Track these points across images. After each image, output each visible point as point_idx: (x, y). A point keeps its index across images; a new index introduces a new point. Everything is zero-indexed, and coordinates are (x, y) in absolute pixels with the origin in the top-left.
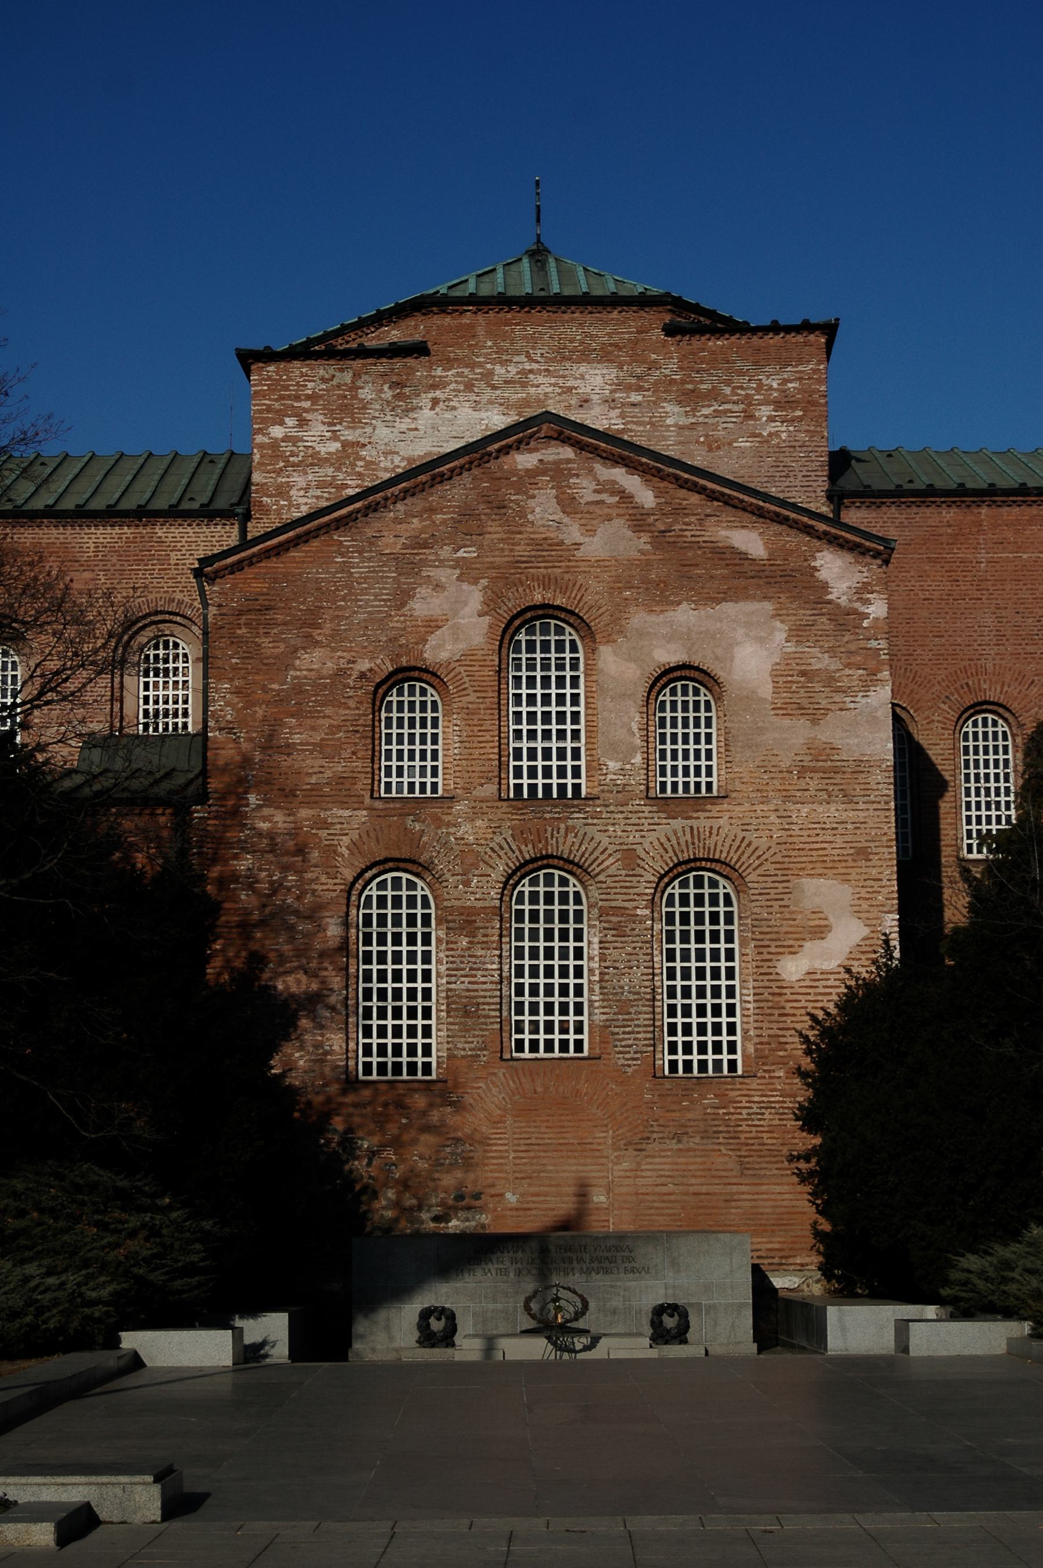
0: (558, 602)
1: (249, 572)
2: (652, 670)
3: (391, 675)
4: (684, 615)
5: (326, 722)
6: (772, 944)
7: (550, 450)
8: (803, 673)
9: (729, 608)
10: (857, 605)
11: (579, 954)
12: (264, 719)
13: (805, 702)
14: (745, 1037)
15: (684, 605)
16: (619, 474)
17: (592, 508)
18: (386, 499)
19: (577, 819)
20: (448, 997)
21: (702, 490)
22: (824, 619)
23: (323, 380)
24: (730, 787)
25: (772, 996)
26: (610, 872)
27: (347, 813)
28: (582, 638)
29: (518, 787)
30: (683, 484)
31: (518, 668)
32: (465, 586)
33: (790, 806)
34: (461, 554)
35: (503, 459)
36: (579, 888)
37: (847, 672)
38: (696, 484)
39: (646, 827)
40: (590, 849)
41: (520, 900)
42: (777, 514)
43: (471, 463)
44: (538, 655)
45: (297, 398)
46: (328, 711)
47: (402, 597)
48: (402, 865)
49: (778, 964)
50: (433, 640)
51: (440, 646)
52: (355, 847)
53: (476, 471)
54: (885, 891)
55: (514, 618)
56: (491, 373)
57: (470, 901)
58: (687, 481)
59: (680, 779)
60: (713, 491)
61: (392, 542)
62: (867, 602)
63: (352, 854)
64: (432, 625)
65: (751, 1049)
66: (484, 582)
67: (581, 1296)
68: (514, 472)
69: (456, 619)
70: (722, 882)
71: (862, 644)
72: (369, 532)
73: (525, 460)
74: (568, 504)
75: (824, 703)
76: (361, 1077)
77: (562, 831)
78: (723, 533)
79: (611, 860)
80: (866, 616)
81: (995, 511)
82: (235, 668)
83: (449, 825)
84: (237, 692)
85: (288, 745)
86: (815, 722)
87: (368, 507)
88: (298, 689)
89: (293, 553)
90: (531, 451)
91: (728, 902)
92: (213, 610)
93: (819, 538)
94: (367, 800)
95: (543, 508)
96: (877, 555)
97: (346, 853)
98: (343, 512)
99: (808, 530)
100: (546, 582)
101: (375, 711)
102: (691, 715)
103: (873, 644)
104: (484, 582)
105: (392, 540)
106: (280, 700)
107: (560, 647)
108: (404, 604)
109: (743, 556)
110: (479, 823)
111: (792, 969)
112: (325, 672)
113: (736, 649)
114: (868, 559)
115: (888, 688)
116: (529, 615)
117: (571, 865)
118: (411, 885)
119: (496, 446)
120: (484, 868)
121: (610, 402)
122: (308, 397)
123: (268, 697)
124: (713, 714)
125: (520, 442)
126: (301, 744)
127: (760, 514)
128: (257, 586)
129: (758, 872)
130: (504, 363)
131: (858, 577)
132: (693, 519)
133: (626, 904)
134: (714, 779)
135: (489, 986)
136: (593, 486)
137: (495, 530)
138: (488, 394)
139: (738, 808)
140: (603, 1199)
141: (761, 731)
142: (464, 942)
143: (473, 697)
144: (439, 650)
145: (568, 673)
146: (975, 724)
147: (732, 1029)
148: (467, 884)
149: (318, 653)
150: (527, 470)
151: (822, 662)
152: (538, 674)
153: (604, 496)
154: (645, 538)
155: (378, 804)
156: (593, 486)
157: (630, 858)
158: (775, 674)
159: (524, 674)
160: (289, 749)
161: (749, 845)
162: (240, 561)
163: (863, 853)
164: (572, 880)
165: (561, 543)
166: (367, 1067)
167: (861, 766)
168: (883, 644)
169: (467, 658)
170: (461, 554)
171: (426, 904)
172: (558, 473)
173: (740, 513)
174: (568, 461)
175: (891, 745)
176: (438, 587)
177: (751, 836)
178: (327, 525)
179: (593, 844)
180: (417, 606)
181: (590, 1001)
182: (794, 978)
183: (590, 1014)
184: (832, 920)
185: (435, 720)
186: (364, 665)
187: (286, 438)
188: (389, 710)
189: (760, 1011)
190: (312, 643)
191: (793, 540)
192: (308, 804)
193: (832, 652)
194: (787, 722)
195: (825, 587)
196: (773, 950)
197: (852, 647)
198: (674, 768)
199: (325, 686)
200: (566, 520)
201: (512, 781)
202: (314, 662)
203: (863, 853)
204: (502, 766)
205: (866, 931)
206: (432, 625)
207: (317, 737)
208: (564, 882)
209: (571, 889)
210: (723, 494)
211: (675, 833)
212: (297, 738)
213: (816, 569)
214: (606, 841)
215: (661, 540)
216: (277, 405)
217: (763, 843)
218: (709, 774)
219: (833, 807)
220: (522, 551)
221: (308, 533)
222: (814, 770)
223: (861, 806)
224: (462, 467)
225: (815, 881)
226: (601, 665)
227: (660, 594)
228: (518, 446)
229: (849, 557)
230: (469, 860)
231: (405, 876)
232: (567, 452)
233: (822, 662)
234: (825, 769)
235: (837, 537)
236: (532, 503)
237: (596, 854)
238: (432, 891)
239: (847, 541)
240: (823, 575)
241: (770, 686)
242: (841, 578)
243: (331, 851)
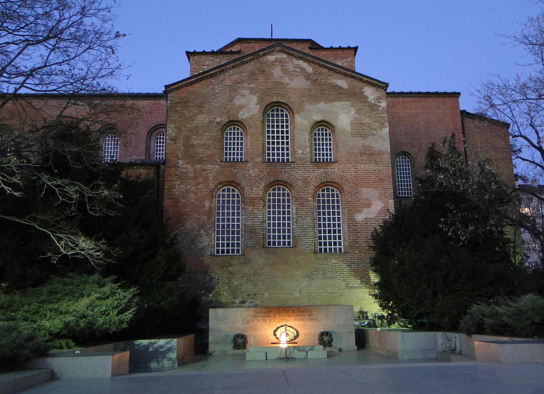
0: (282, 101)
1: (182, 90)
2: (312, 122)
3: (227, 123)
4: (322, 105)
5: (206, 138)
6: (353, 209)
7: (280, 55)
8: (361, 124)
9: (337, 104)
10: (377, 103)
11: (289, 213)
12: (185, 136)
13: (361, 133)
14: (345, 240)
15: (322, 103)
16: (301, 63)
17: (294, 73)
18: (226, 68)
19: (288, 169)
20: (245, 227)
21: (327, 68)
22: (367, 107)
23: (211, 61)
24: (338, 159)
25: (354, 227)
26: (299, 186)
27: (212, 166)
28: (289, 113)
29: (269, 159)
30: (321, 66)
31: (269, 122)
32: (252, 96)
33: (357, 165)
34: (250, 86)
35: (264, 57)
36: (289, 192)
37: (375, 123)
38: (325, 66)
39: (311, 171)
40: (293, 178)
41: (269, 195)
42: (351, 75)
43: (254, 58)
44: (275, 118)
45: (203, 65)
46: (207, 134)
47: (231, 99)
48: (230, 184)
49: (355, 216)
50: (241, 112)
51: (244, 114)
52: (215, 178)
53: (256, 61)
54: (389, 192)
55: (267, 106)
57: (253, 195)
58: (322, 65)
60: (331, 68)
61: (228, 82)
62: (380, 102)
63: (213, 179)
64: (241, 107)
65: (347, 244)
66: (258, 94)
67: (296, 330)
68: (267, 61)
69: (249, 106)
70: (335, 190)
71: (379, 115)
72: (221, 78)
73: (271, 58)
74: (285, 71)
75: (367, 133)
76: (216, 254)
77: (283, 172)
78: (334, 81)
79: (300, 182)
80: (380, 106)
81: (404, 99)
82: (176, 120)
83: (246, 170)
84: (176, 128)
85: (193, 145)
86: (365, 139)
87: (221, 71)
88: (197, 127)
90: (273, 55)
91: (338, 196)
92: (169, 102)
93: (364, 83)
94: (219, 162)
95: (277, 72)
96: (383, 88)
97: (211, 179)
98: (213, 72)
99: (361, 80)
100: (278, 95)
101: (222, 134)
102: (325, 137)
103: (382, 115)
104: (258, 94)
105: (228, 81)
106: (191, 130)
107: (282, 116)
108: (232, 101)
109: (341, 88)
111: (360, 217)
112: (205, 122)
113: (339, 116)
114: (380, 89)
115: (388, 129)
116: (272, 105)
117: (286, 184)
118: (233, 191)
119: (262, 53)
120: (257, 184)
122: (207, 65)
123: (187, 129)
124: (331, 137)
125: (269, 52)
126: (197, 144)
127: (346, 75)
128: (184, 95)
129: (348, 185)
131: (377, 95)
132: (324, 76)
133: (305, 196)
134: (332, 157)
135: (259, 223)
136: (293, 66)
137: (261, 79)
139: (341, 166)
140: (298, 295)
142: (251, 208)
143: (254, 130)
144: (243, 115)
145: (285, 124)
146: (400, 158)
147: (340, 238)
148: (252, 189)
149: (204, 116)
150: (272, 61)
151: (367, 120)
153: (296, 69)
154: (309, 82)
155: (223, 164)
156: (293, 66)
157: (306, 181)
158: (351, 124)
159: (271, 124)
160: (193, 146)
161: (345, 177)
162: (178, 87)
163: (381, 180)
164: (287, 189)
165: (283, 83)
166: (218, 251)
167: (380, 153)
168: (386, 115)
169: (251, 118)
170: (250, 86)
171: (238, 197)
172: (281, 62)
173: (340, 75)
174: (285, 58)
175: (389, 146)
176: (243, 96)
177: (345, 174)
178: (207, 76)
179: (294, 177)
180: (236, 101)
181: (293, 228)
182: (360, 220)
183: (293, 233)
184: (372, 202)
185: (242, 138)
186: (218, 120)
188: (227, 135)
189: (349, 232)
190: (201, 112)
192: (200, 163)
193: (369, 117)
194: (356, 139)
195: (367, 97)
196: (353, 211)
197: (376, 116)
198: (319, 154)
199: (205, 126)
200: (284, 76)
201: (267, 158)
202: (202, 119)
203: (381, 180)
204: (264, 152)
205: (383, 205)
206: (241, 107)
207: (203, 142)
208: (284, 190)
209: (286, 192)
210: (334, 69)
211: (320, 173)
212: (196, 142)
213: (363, 92)
214: (298, 176)
215: (315, 82)
216: (197, 67)
217: (349, 177)
218: (331, 156)
219: (371, 165)
220: (270, 85)
221: (201, 78)
223: (380, 165)
224: (251, 59)
226: (295, 120)
227: (315, 99)
228: (269, 53)
229: (374, 89)
230: (253, 182)
231: (231, 188)
232: (285, 56)
233: (367, 120)
234: (369, 154)
235: (370, 82)
236: (273, 71)
237: (295, 180)
238: (240, 192)
239: (374, 84)
240: (366, 94)
241: (350, 128)
242: (371, 95)
243: (207, 179)
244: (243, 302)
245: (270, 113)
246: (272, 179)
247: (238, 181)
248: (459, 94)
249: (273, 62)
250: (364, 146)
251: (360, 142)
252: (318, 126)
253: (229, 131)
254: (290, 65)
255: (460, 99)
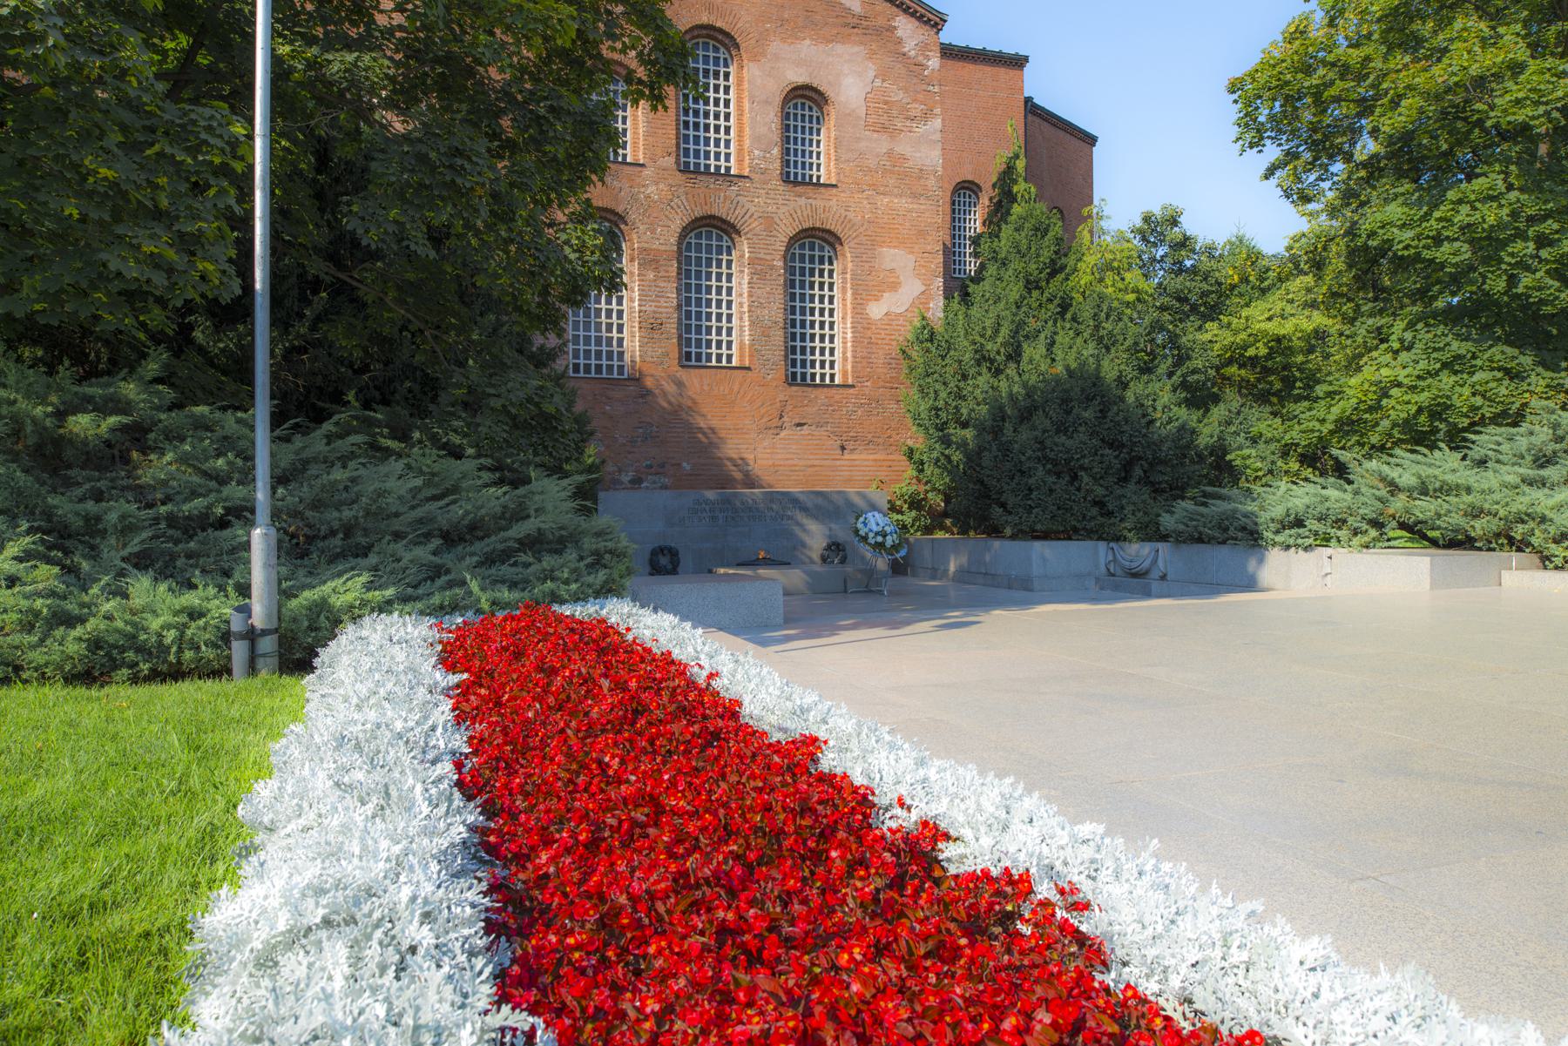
0: (718, 25)
4: (806, 48)
6: (864, 293)
8: (886, 103)
15: (808, 42)
59: (799, 171)
100: (710, 8)
110: (661, 186)
111: (876, 311)
141: (858, 140)
142: (651, 275)
157: (769, 222)
163: (922, 234)
177: (851, 215)
193: (906, 90)
194: (875, 135)
195: (900, 41)
203: (922, 234)
214: (753, 209)
222: (892, 172)
225: (892, 251)
234: (898, 171)
240: (899, 33)
244: (637, 482)
246: (698, 213)
247: (620, 209)
248: (1026, 59)
250: (890, 153)
251: (882, 144)
252: (796, 97)
255: (1028, 69)
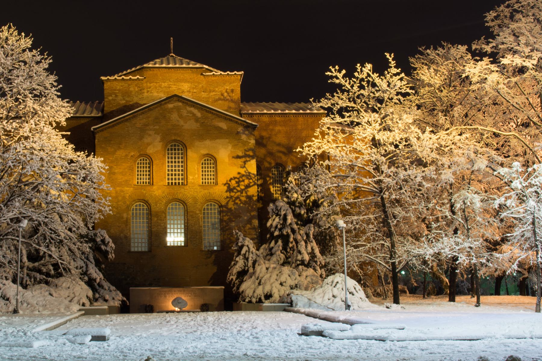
16: (192, 109)
27: (128, 189)
34: (155, 127)
46: (124, 164)
50: (149, 148)
53: (159, 108)
56: (161, 85)
73: (170, 106)
74: (181, 116)
80: (250, 143)
89: (116, 127)
95: (174, 116)
99: (236, 122)
109: (221, 129)
121: (189, 92)
127: (225, 119)
130: (164, 82)
138: (161, 90)
142: (156, 219)
148: (156, 205)
152: (173, 156)
154: (199, 124)
155: (136, 187)
160: (114, 173)
170: (155, 127)
172: (178, 109)
176: (150, 135)
187: (112, 100)
191: (233, 125)
200: (180, 120)
207: (121, 171)
212: (116, 171)
228: (168, 102)
232: (180, 104)
245: (170, 148)
249: (172, 109)
253: (139, 162)
254: (184, 111)
